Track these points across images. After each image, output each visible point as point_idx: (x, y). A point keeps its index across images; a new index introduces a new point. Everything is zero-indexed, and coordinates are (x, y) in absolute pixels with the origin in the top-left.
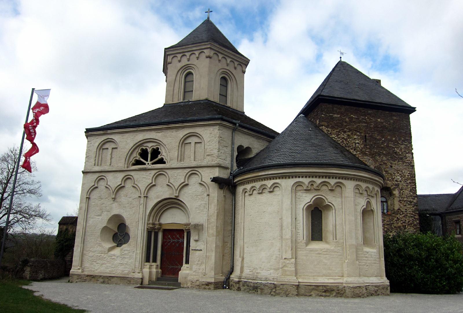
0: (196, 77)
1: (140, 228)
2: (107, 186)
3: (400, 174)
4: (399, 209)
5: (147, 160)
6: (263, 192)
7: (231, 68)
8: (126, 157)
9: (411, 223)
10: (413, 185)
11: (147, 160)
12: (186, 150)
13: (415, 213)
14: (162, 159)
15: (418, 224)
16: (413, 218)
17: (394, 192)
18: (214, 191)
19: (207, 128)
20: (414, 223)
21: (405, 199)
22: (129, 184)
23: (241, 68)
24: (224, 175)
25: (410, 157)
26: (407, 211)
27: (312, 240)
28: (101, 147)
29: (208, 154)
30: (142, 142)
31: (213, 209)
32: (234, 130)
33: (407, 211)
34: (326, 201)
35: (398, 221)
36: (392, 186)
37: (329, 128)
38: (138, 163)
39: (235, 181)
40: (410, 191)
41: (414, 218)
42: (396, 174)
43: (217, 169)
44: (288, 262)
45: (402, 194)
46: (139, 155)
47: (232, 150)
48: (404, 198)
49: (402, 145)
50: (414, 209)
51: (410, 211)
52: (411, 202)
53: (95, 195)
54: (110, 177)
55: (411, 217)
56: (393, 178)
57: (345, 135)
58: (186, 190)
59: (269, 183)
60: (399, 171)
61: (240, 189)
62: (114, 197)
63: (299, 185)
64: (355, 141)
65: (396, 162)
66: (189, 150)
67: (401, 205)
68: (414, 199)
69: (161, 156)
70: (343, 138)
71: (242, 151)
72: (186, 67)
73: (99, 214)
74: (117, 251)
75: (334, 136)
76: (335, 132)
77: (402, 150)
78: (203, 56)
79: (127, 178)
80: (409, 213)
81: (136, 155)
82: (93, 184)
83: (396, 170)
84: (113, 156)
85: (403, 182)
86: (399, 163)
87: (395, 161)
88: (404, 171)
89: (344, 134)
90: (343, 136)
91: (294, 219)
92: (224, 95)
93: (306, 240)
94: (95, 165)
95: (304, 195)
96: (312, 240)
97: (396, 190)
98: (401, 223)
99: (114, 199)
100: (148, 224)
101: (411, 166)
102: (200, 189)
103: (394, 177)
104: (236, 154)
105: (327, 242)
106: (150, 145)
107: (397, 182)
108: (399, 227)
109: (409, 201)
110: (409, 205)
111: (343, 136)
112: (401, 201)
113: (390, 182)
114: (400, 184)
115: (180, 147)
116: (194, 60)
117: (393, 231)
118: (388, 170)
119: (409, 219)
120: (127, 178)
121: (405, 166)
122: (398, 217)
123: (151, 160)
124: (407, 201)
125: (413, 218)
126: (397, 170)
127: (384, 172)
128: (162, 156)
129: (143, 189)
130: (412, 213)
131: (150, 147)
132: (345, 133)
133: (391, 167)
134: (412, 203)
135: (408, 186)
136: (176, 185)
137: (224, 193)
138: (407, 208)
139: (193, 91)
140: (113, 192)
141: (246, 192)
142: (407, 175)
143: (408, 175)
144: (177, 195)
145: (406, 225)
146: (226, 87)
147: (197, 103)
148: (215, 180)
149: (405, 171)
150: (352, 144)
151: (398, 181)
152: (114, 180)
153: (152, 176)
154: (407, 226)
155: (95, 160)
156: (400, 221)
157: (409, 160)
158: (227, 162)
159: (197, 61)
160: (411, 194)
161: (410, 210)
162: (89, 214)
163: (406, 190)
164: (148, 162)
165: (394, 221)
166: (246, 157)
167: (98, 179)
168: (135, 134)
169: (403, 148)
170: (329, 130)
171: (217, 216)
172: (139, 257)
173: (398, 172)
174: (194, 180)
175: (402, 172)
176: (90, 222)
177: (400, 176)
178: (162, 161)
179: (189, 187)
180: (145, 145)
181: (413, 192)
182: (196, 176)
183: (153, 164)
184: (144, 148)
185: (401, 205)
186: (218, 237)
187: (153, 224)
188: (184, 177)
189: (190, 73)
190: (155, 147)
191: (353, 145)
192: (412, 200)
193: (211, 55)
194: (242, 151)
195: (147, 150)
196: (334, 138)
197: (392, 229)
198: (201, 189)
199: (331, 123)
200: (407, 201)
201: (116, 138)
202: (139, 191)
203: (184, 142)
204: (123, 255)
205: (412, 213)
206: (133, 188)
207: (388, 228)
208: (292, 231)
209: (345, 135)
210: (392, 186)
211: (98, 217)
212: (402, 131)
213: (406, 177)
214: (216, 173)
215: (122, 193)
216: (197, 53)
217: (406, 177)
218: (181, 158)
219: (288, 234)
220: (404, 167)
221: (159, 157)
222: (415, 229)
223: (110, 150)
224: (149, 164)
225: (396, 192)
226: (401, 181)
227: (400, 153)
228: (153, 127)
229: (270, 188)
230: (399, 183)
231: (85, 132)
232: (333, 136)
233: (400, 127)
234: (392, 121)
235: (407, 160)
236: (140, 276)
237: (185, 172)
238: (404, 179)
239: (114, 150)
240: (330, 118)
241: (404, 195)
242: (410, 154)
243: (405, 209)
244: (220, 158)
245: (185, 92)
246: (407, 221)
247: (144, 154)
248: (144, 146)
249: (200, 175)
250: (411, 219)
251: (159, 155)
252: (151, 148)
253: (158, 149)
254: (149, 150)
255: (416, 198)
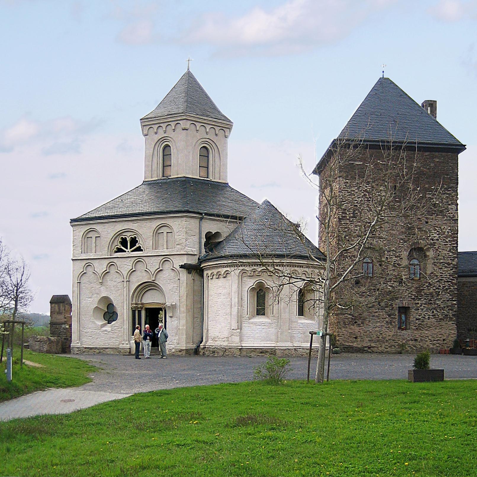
0: (173, 151)
1: (125, 308)
2: (95, 272)
3: (437, 231)
4: (432, 273)
5: (127, 248)
6: (220, 277)
7: (212, 136)
8: (108, 246)
9: (446, 288)
10: (454, 244)
11: (127, 248)
12: (159, 239)
13: (452, 277)
14: (140, 247)
15: (455, 290)
16: (450, 283)
17: (428, 254)
18: (184, 275)
19: (175, 219)
20: (451, 288)
21: (441, 261)
22: (113, 270)
23: (224, 133)
24: (193, 261)
25: (453, 209)
26: (442, 275)
27: (257, 315)
28: (86, 236)
29: (177, 243)
30: (121, 232)
31: (183, 290)
32: (201, 219)
33: (442, 275)
34: (266, 285)
35: (429, 287)
36: (426, 245)
37: (347, 180)
38: (119, 250)
39: (201, 266)
40: (450, 251)
41: (451, 283)
42: (433, 231)
43: (186, 256)
44: (235, 331)
45: (438, 256)
46: (119, 243)
47: (200, 238)
48: (441, 259)
49: (444, 194)
50: (451, 272)
51: (446, 275)
52: (449, 264)
53: (84, 279)
54: (96, 263)
55: (448, 281)
56: (429, 235)
57: (368, 187)
58: (160, 274)
59: (223, 270)
60: (437, 227)
61: (205, 273)
62: (101, 281)
63: (243, 272)
64: (381, 193)
65: (434, 216)
66: (163, 239)
67: (435, 268)
68: (453, 260)
69: (138, 244)
70: (366, 191)
71: (210, 236)
72: (163, 139)
73: (90, 296)
74: (108, 328)
75: (354, 189)
76: (355, 184)
77: (443, 200)
78: (179, 128)
79: (111, 265)
80: (445, 278)
81: (118, 244)
82: (82, 270)
83: (434, 226)
84: (97, 244)
85: (440, 240)
86: (437, 217)
87: (431, 216)
88: (443, 227)
89: (367, 186)
90: (366, 188)
91: (240, 299)
92: (205, 166)
93: (250, 315)
94: (82, 253)
95: (249, 280)
96: (257, 315)
97: (431, 250)
98: (433, 289)
99: (101, 283)
100: (131, 304)
101: (453, 220)
102: (173, 274)
103: (430, 235)
104: (204, 240)
105: (268, 317)
106: (128, 234)
107: (433, 240)
108: (431, 294)
109: (446, 263)
110: (446, 267)
111: (366, 188)
112: (436, 264)
113: (423, 241)
114: (436, 243)
115: (154, 237)
116: (170, 133)
117: (422, 298)
118: (422, 226)
119: (444, 284)
120: (111, 265)
121: (446, 220)
122: (430, 283)
123: (130, 248)
124: (444, 263)
125: (450, 283)
126: (434, 226)
127: (416, 230)
128: (139, 245)
129: (125, 274)
130: (449, 277)
131: (128, 236)
132: (368, 185)
133: (427, 222)
134: (450, 265)
135: (447, 245)
136: (153, 270)
137: (193, 277)
138: (444, 271)
139: (171, 166)
140: (100, 278)
141: (213, 275)
142: (446, 231)
143: (448, 232)
144: (154, 279)
145: (439, 292)
146: (208, 157)
147: (177, 181)
148: (182, 267)
149: (444, 227)
150: (376, 198)
151: (435, 240)
152: (101, 267)
153: (132, 263)
154: (440, 293)
155: (82, 248)
156: (432, 286)
157: (452, 213)
158: (195, 251)
159: (173, 133)
160: (451, 254)
161: (447, 274)
162: (81, 297)
163: (444, 250)
164: (128, 250)
165: (425, 287)
166: (217, 241)
167: (86, 266)
168: (116, 224)
169: (445, 198)
170: (348, 182)
171: (187, 296)
172: (126, 331)
173: (435, 229)
174: (167, 266)
175: (440, 228)
176: (83, 303)
177: (438, 233)
178: (139, 249)
179: (164, 272)
180: (124, 234)
181: (454, 251)
182: (169, 263)
183: (132, 251)
184: (124, 237)
185: (435, 268)
186: (188, 314)
187: (136, 304)
188: (158, 264)
189: (167, 146)
190: (133, 236)
191: (377, 199)
192: (450, 261)
193: (187, 127)
194: (210, 236)
195: (126, 238)
196: (354, 191)
197: (421, 297)
198: (173, 273)
199: (351, 172)
200: (444, 263)
201: (98, 227)
202: (122, 276)
203: (157, 232)
204: (113, 330)
205: (449, 277)
206: (117, 273)
207: (416, 295)
208: (238, 308)
209: (368, 187)
210: (426, 245)
211: (90, 299)
212: (445, 176)
213: (445, 234)
214: (184, 260)
215: (108, 277)
216: (173, 124)
217: (445, 234)
218: (156, 246)
219: (235, 310)
220: (444, 222)
221: (137, 245)
222: (450, 295)
223: (94, 239)
224: (129, 252)
225: (431, 254)
226: (438, 240)
227: (441, 205)
228: (130, 219)
229: (224, 274)
230: (435, 241)
231: (70, 222)
232: (353, 189)
233: (444, 171)
234: (432, 165)
235: (449, 214)
236: (128, 346)
237: (159, 259)
238: (442, 236)
239: (97, 238)
240: (349, 167)
241: (440, 256)
242: (453, 205)
243: (441, 273)
244: (188, 247)
245: (164, 166)
246: (442, 287)
247: (124, 242)
248: (122, 235)
249: (172, 262)
250: (447, 284)
251: (137, 244)
252: (130, 237)
253: (135, 237)
254: (128, 239)
255: (457, 259)
